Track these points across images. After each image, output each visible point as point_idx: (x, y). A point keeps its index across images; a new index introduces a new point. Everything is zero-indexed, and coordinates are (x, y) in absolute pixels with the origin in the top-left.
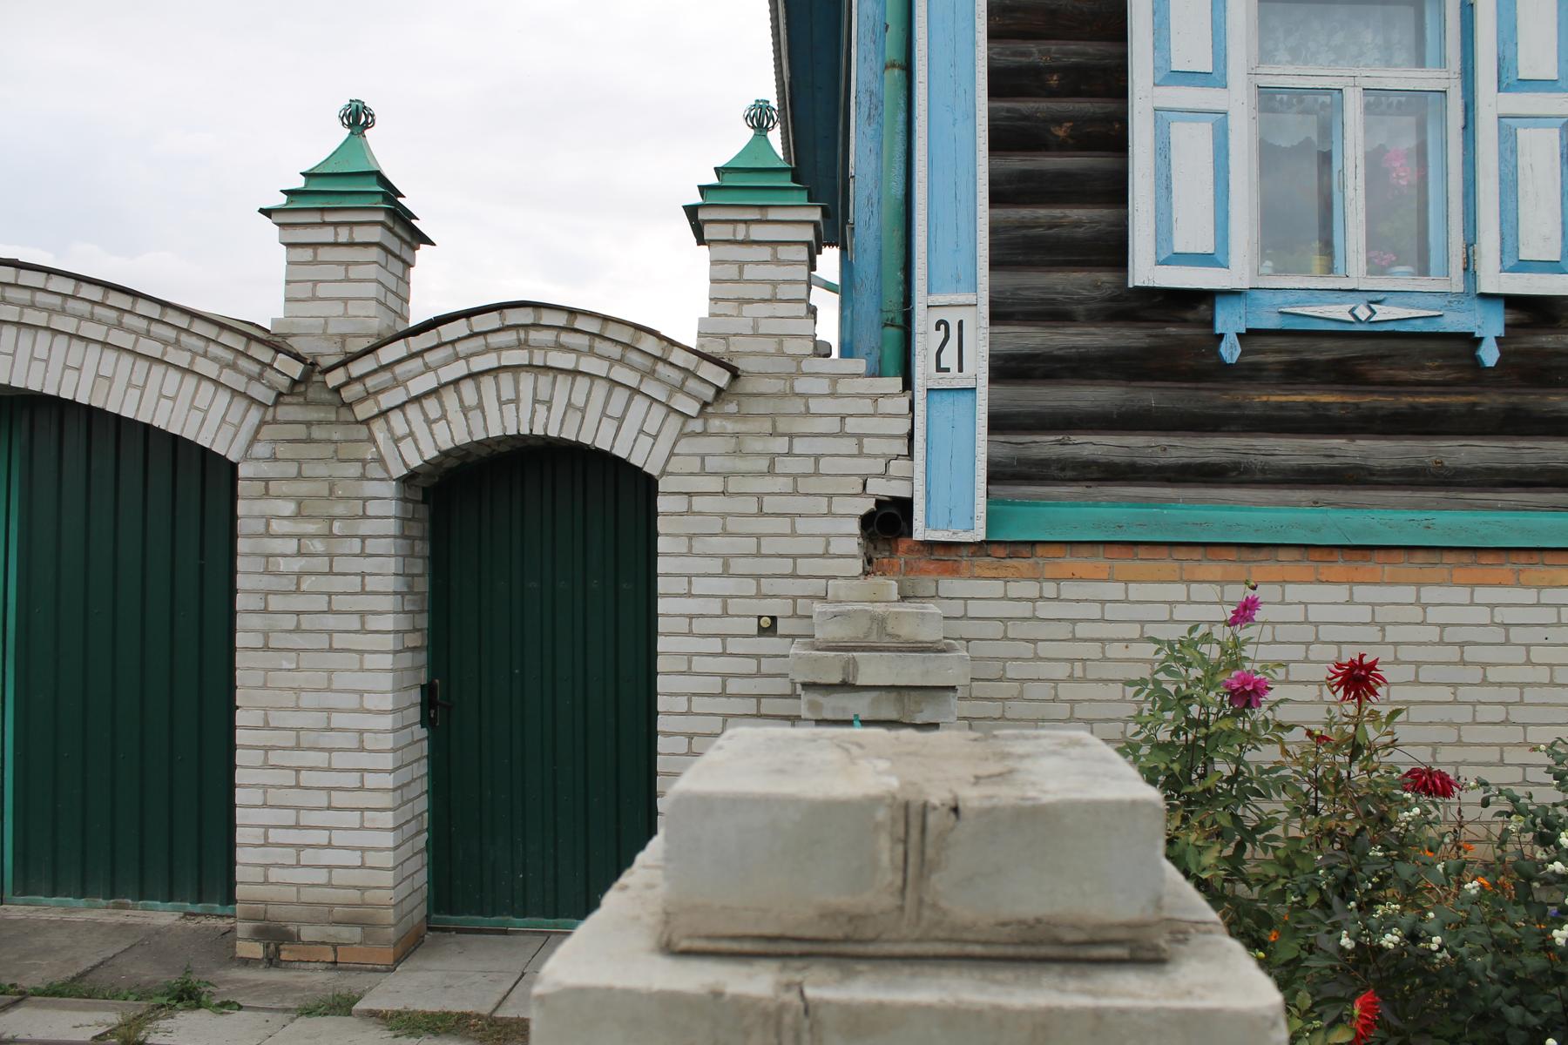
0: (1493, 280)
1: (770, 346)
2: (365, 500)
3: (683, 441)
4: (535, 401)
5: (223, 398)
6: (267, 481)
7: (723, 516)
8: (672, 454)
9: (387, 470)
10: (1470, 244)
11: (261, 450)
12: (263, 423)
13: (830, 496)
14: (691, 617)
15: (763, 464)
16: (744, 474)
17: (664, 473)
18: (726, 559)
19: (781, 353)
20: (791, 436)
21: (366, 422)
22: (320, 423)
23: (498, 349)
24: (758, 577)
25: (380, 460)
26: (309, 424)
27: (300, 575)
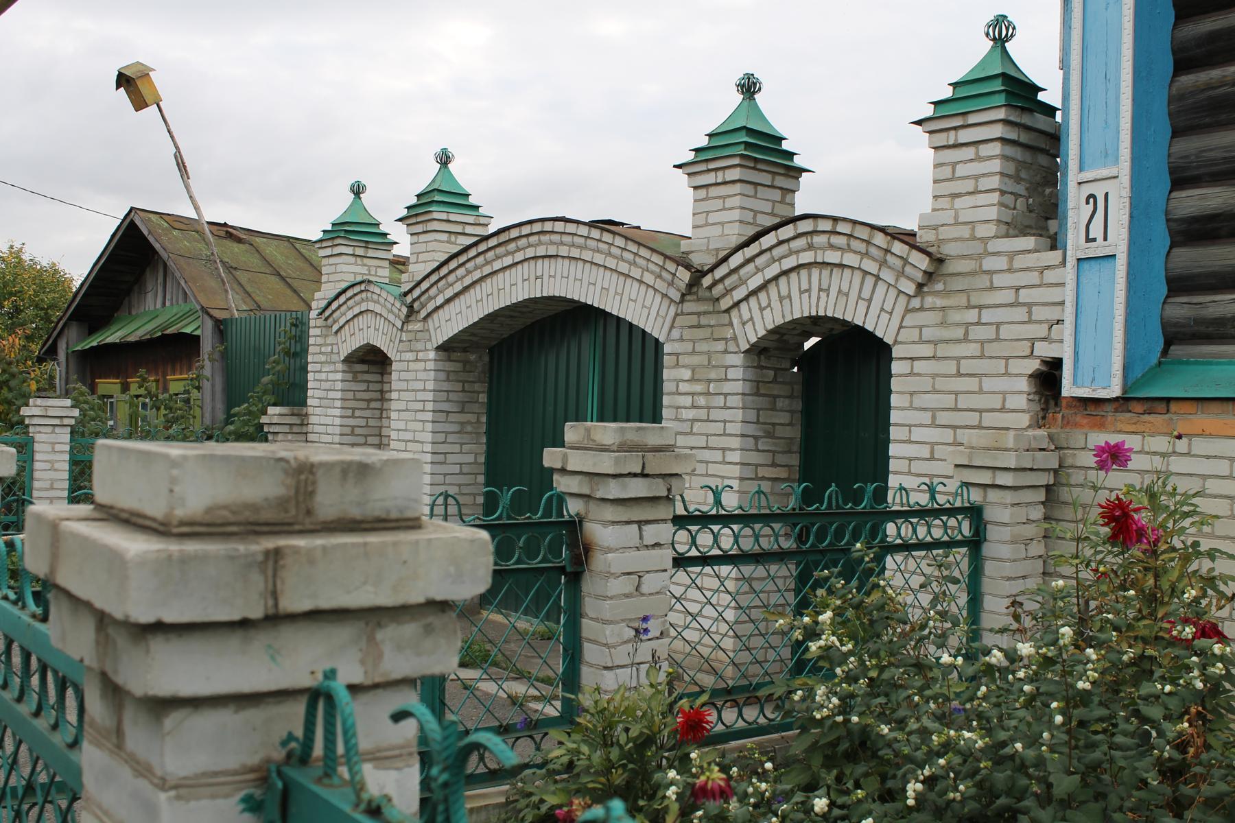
1: (965, 232)
2: (727, 367)
3: (908, 316)
4: (820, 290)
6: (678, 355)
7: (934, 376)
8: (901, 327)
9: (738, 346)
11: (676, 334)
12: (677, 315)
13: (1007, 358)
14: (910, 459)
15: (959, 333)
16: (947, 341)
17: (896, 342)
18: (934, 411)
19: (973, 238)
20: (980, 308)
21: (728, 311)
22: (705, 313)
23: (797, 252)
24: (955, 428)
25: (735, 338)
26: (699, 314)
27: (693, 421)
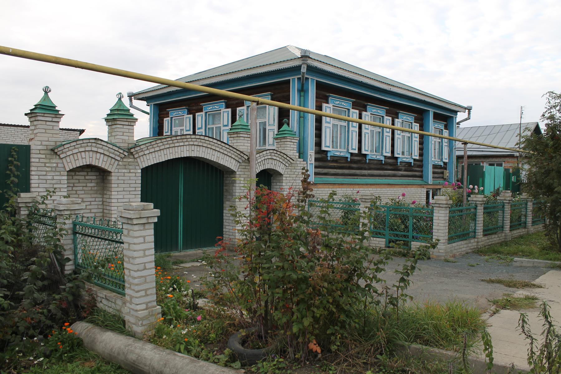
0: (351, 151)
5: (235, 161)
10: (348, 145)
11: (239, 170)
